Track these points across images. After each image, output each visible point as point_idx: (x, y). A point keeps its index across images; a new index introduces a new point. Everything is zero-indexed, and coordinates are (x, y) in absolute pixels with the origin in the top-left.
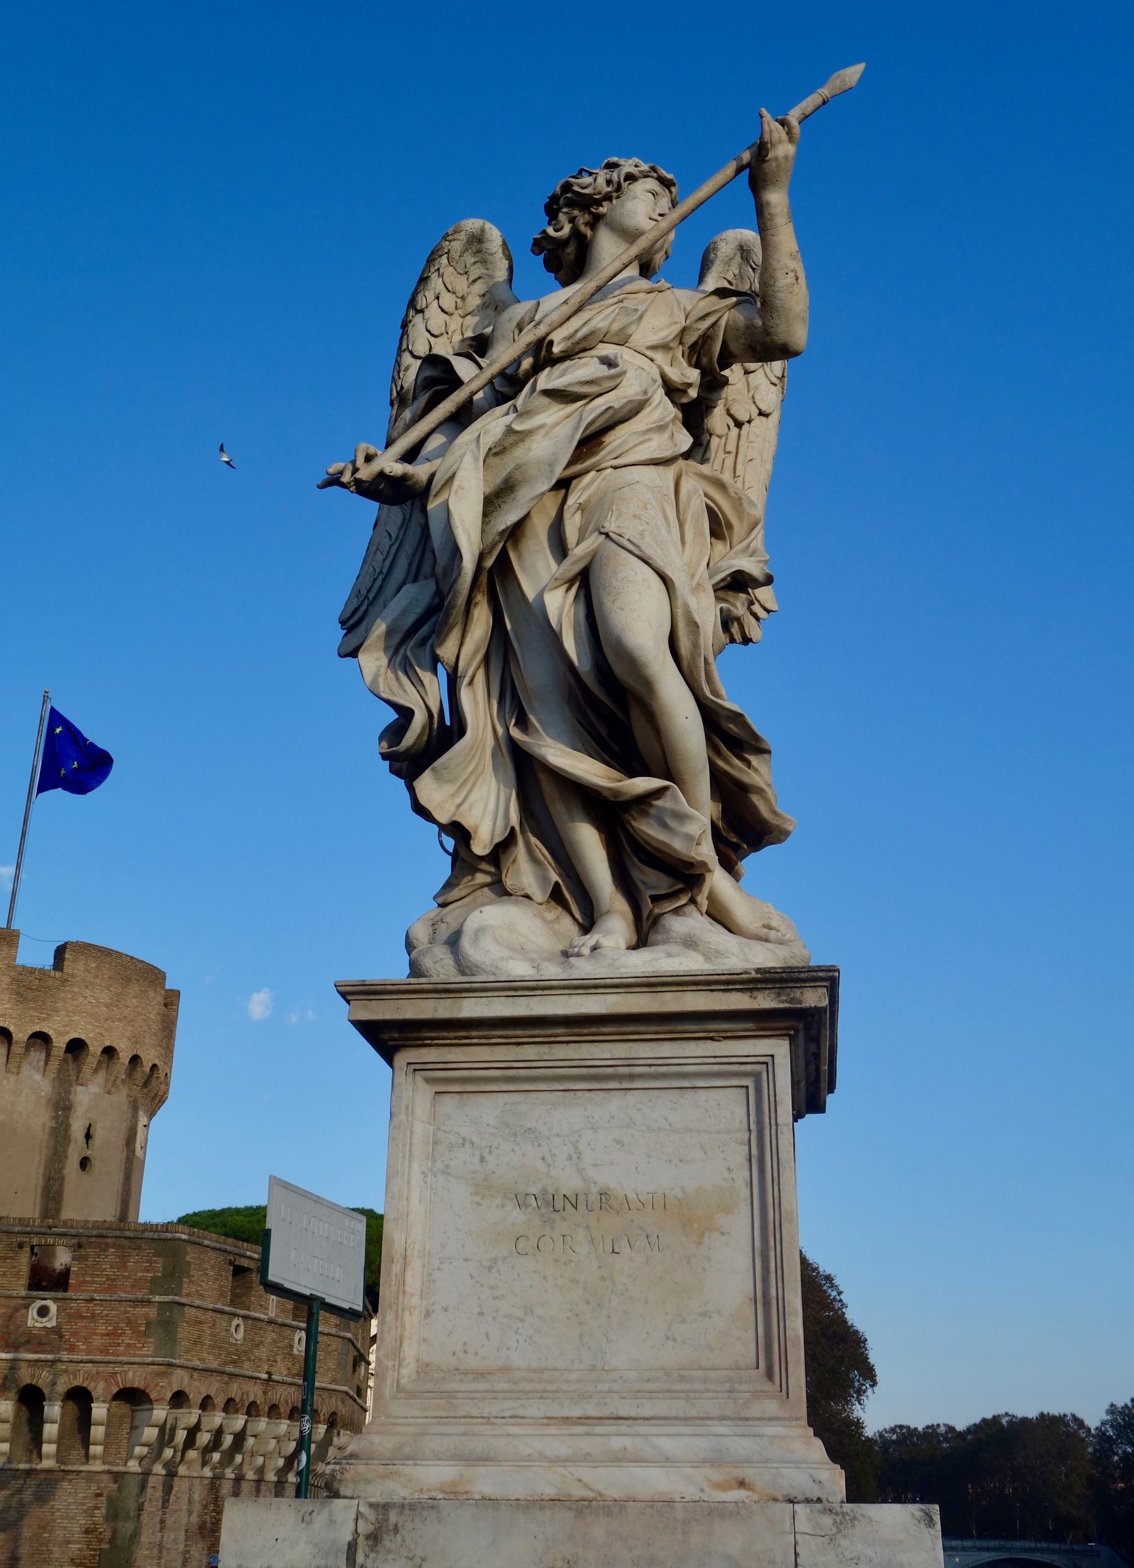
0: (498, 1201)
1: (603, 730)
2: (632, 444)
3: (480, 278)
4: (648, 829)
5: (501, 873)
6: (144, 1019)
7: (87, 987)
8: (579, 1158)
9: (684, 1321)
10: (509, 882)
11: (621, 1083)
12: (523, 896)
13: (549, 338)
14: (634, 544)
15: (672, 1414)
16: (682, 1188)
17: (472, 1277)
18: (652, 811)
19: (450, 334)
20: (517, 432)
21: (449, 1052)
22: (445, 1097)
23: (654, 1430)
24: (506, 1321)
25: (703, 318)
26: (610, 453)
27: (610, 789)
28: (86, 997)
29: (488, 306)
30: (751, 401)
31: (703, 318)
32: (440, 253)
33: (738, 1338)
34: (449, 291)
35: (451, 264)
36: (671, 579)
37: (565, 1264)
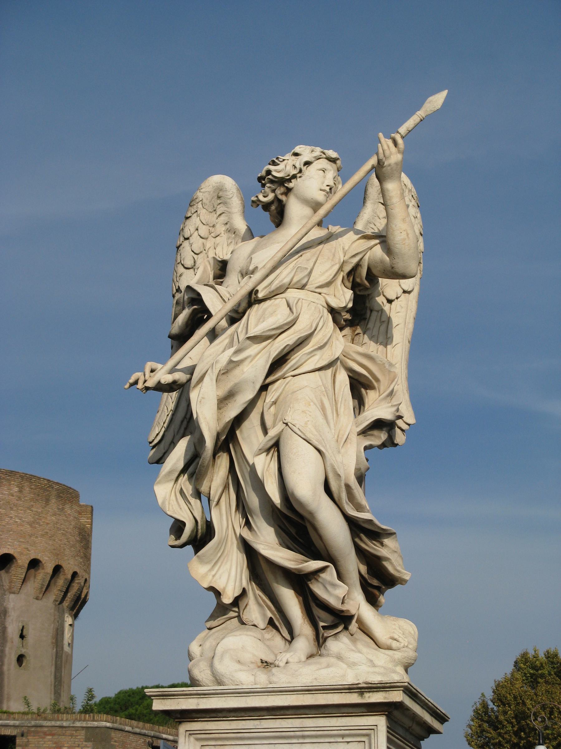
1: (293, 531)
2: (303, 361)
6: (63, 534)
7: (11, 509)
10: (245, 617)
11: (298, 740)
12: (253, 625)
13: (256, 289)
14: (301, 431)
19: (207, 250)
20: (234, 362)
21: (207, 724)
25: (354, 256)
26: (290, 368)
27: (295, 569)
28: (11, 517)
29: (229, 231)
31: (354, 256)
34: (204, 224)
35: (204, 208)
36: (323, 452)
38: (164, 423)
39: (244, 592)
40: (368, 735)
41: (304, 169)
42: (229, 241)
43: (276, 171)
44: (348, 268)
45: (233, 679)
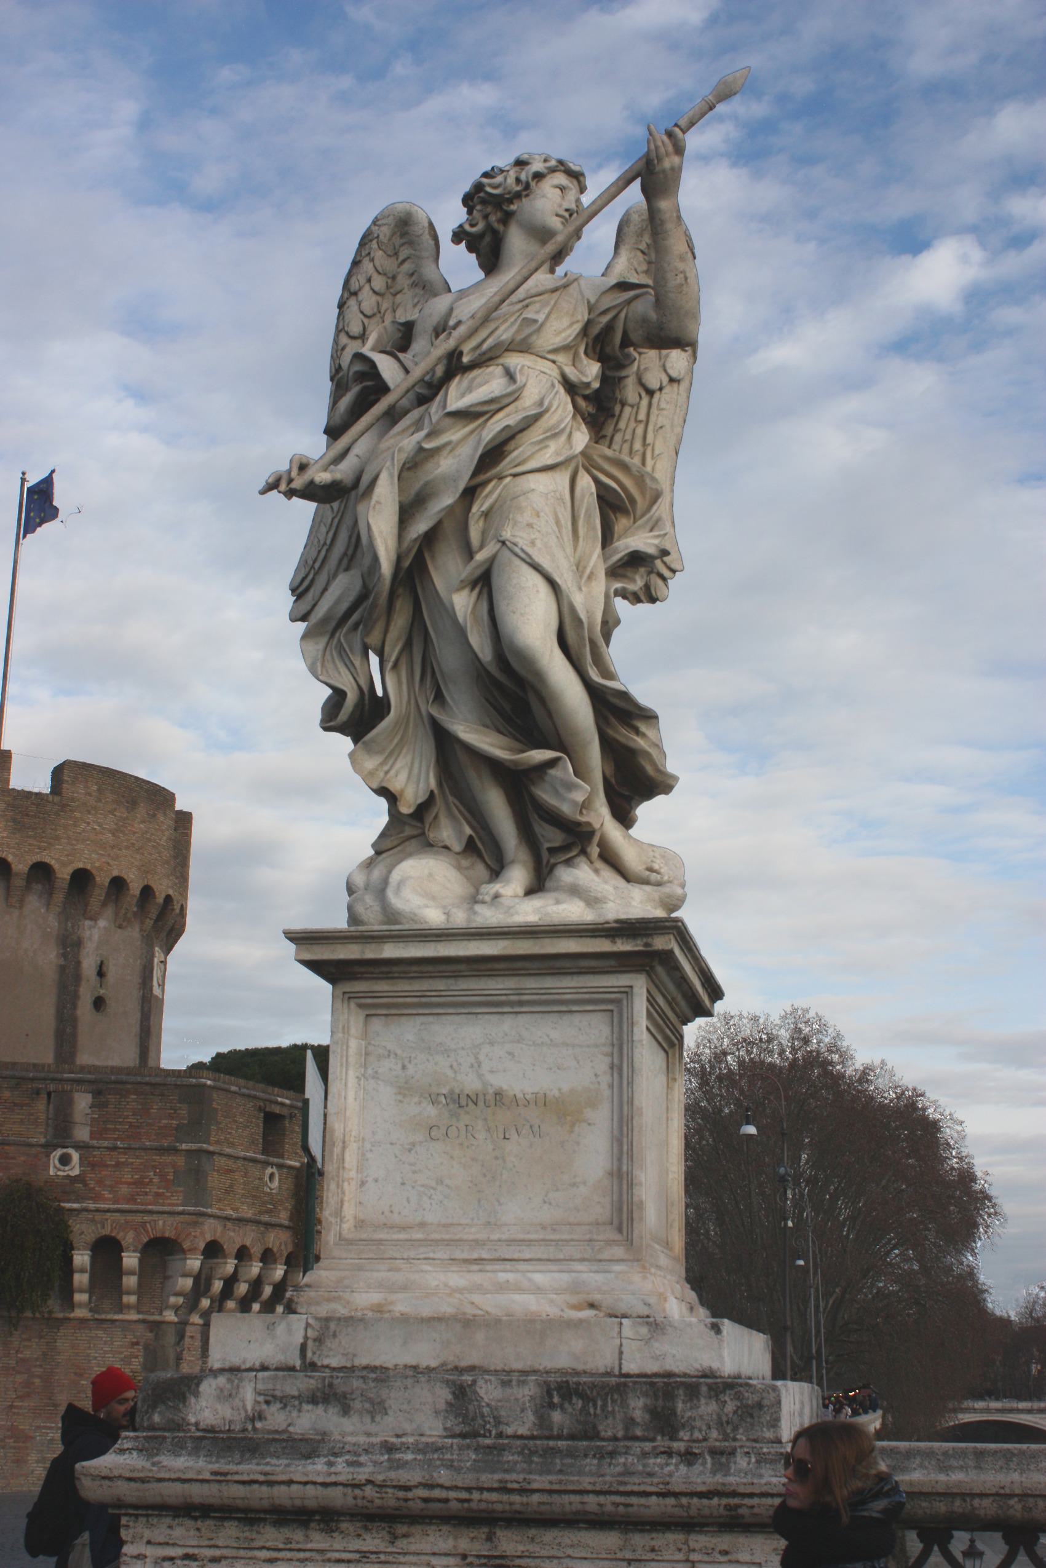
0: (416, 1099)
2: (529, 453)
3: (408, 258)
4: (545, 795)
5: (424, 827)
6: (153, 846)
7: (89, 812)
8: (479, 1066)
9: (557, 1190)
10: (431, 836)
15: (545, 1256)
16: (560, 1090)
17: (396, 1157)
18: (547, 778)
22: (374, 1020)
23: (530, 1268)
24: (422, 1189)
25: (604, 312)
26: (511, 462)
27: (512, 761)
28: (88, 823)
29: (416, 285)
30: (661, 369)
31: (604, 312)
32: (370, 237)
33: (599, 1202)
36: (558, 585)
37: (468, 1147)
38: (314, 562)
39: (431, 798)
40: (618, 1002)
41: (533, 184)
42: (416, 300)
43: (490, 185)
44: (595, 330)
45: (416, 918)
